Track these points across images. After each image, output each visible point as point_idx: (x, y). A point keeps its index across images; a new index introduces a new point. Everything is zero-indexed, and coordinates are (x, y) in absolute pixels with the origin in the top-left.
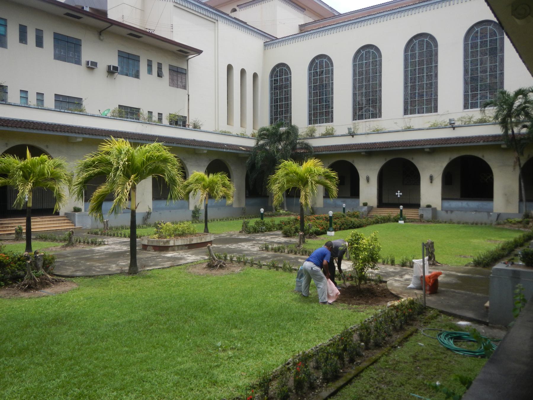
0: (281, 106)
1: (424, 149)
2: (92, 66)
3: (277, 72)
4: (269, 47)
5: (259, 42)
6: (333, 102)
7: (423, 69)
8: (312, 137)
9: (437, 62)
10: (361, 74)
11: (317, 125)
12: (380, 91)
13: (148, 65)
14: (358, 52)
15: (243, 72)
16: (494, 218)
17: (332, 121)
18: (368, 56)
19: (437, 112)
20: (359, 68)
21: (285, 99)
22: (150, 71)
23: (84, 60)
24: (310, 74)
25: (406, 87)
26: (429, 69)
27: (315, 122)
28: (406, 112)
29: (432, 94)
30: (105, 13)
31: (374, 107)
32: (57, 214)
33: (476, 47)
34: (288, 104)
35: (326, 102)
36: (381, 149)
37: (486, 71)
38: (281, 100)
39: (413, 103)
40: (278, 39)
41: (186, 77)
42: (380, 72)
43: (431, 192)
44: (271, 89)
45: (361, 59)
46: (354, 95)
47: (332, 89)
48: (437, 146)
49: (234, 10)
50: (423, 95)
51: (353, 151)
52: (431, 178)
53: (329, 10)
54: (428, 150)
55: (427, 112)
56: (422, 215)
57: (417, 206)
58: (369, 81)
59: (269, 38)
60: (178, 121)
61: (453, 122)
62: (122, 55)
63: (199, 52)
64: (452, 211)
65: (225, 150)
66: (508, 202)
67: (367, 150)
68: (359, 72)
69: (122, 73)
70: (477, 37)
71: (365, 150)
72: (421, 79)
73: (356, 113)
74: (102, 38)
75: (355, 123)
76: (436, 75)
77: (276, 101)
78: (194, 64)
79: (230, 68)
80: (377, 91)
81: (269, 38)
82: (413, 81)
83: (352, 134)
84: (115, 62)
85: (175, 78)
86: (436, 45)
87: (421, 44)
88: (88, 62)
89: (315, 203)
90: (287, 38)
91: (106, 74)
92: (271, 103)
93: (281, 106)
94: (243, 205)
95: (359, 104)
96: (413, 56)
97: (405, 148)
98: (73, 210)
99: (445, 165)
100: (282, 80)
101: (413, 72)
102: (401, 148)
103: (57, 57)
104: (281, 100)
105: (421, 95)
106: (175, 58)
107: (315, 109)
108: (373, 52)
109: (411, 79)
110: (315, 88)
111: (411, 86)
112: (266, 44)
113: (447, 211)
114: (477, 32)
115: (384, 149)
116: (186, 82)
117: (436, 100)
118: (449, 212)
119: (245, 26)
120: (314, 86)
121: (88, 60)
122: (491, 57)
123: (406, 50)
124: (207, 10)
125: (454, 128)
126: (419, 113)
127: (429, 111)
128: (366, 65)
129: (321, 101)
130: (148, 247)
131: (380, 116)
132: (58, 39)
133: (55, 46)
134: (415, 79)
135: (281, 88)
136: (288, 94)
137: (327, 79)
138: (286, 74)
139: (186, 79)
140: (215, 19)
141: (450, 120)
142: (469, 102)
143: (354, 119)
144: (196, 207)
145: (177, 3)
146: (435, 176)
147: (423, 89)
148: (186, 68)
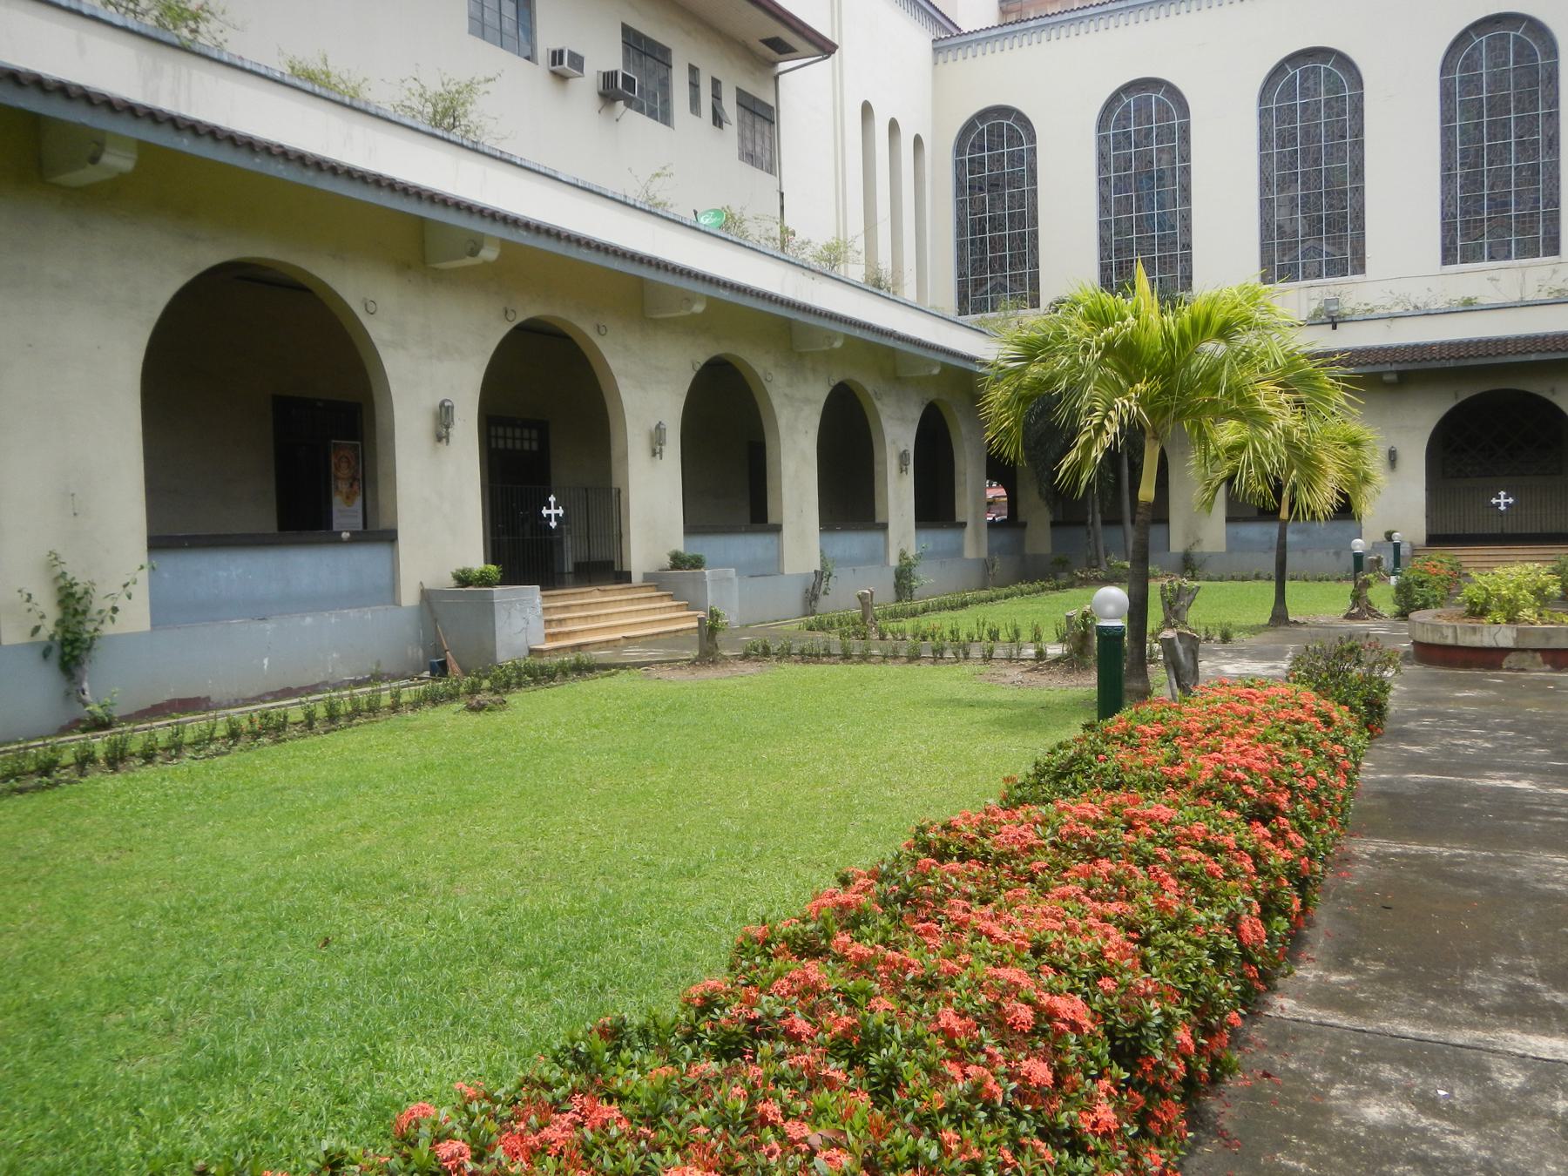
0: (997, 244)
2: (563, 66)
3: (981, 134)
4: (950, 56)
5: (917, 38)
9: (1554, 102)
10: (1286, 138)
12: (1359, 191)
14: (1279, 70)
15: (893, 126)
18: (1310, 83)
20: (1280, 121)
21: (1011, 221)
24: (1102, 140)
25: (1447, 178)
28: (1448, 255)
31: (1338, 243)
32: (624, 577)
34: (1022, 237)
35: (1161, 228)
36: (1462, 363)
38: (997, 223)
42: (1359, 132)
44: (959, 188)
45: (1288, 92)
46: (1265, 205)
47: (1186, 189)
50: (1506, 204)
55: (1519, 256)
58: (1317, 161)
59: (948, 31)
63: (826, 48)
67: (1410, 367)
68: (1279, 132)
71: (1393, 368)
72: (1500, 154)
78: (801, 88)
79: (867, 109)
81: (948, 31)
85: (748, 134)
86: (1551, 49)
87: (1498, 47)
88: (557, 57)
89: (1198, 541)
91: (593, 101)
92: (961, 231)
93: (997, 244)
94: (984, 554)
95: (1282, 234)
96: (1471, 84)
98: (667, 562)
101: (1472, 134)
102: (1533, 357)
104: (997, 223)
108: (1329, 73)
110: (1122, 184)
111: (1466, 177)
112: (940, 44)
115: (1471, 362)
117: (1554, 219)
121: (557, 47)
123: (1446, 68)
126: (1492, 258)
127: (1528, 250)
128: (1304, 110)
130: (1510, 660)
131: (1360, 268)
135: (995, 185)
136: (1022, 206)
137: (1165, 157)
138: (1015, 139)
144: (903, 555)
148: (773, 104)
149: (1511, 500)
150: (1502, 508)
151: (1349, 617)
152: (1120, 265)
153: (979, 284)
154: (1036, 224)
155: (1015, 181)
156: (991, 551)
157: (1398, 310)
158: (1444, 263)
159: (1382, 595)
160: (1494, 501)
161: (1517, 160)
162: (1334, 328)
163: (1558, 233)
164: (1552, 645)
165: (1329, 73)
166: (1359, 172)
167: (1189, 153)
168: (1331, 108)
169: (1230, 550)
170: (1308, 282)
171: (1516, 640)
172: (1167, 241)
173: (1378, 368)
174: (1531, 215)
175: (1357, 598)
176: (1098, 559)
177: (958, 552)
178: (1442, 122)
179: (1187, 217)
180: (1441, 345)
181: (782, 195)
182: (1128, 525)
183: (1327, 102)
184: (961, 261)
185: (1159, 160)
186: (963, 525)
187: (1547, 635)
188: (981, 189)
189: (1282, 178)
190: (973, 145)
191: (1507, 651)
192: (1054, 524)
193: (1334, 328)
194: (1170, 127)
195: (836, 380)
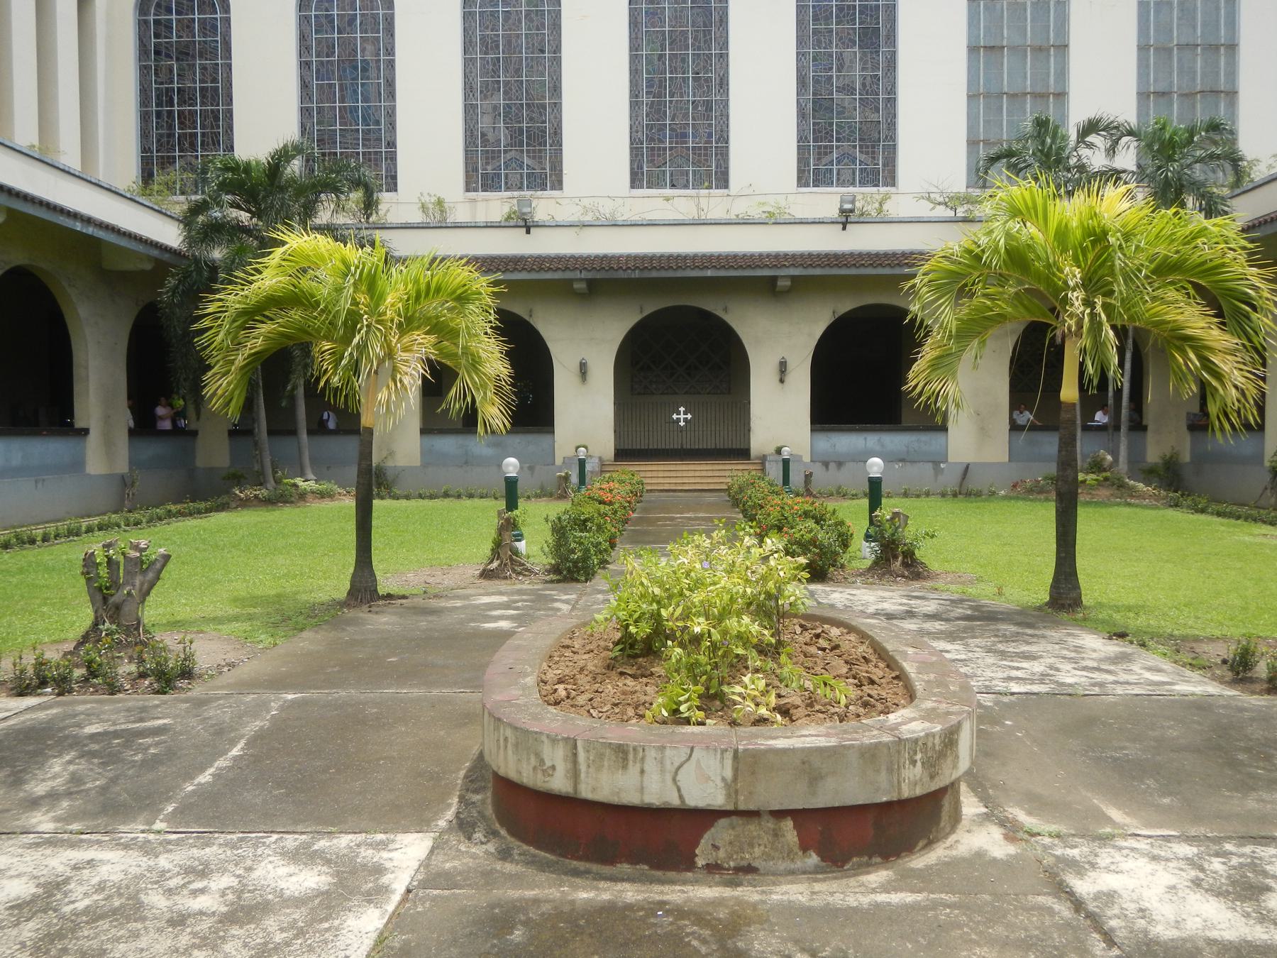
1: (774, 279)
7: (684, 60)
9: (725, 45)
10: (489, 45)
12: (557, 107)
16: (950, 479)
19: (726, 187)
21: (203, 96)
25: (634, 105)
26: (704, 61)
28: (636, 180)
29: (710, 135)
31: (537, 156)
33: (828, 19)
36: (646, 275)
37: (848, 89)
38: (186, 96)
39: (656, 154)
42: (557, 49)
43: (779, 410)
46: (469, 110)
47: (391, 84)
48: (818, 272)
50: (685, 135)
51: (549, 276)
52: (783, 367)
54: (788, 283)
56: (811, 474)
57: (743, 453)
58: (518, 72)
64: (840, 464)
66: (983, 431)
68: (483, 38)
72: (679, 87)
75: (474, 200)
76: (724, 83)
77: (165, 97)
80: (544, 106)
82: (655, 89)
94: (122, 467)
95: (485, 142)
97: (722, 273)
99: (819, 330)
102: (709, 273)
109: (650, 83)
113: (826, 465)
115: (654, 274)
117: (724, 154)
118: (832, 466)
122: (864, 54)
126: (673, 186)
127: (702, 181)
128: (506, 19)
131: (558, 184)
134: (662, 83)
135: (184, 53)
136: (215, 80)
137: (369, 47)
142: (813, 171)
146: (791, 366)
147: (686, 116)
149: (689, 416)
150: (682, 424)
151: (486, 574)
155: (208, 51)
156: (131, 463)
157: (588, 218)
158: (632, 187)
159: (534, 546)
160: (675, 416)
161: (694, 96)
162: (528, 232)
163: (727, 168)
164: (825, 797)
166: (556, 89)
167: (393, 48)
168: (531, 21)
169: (425, 465)
170: (509, 194)
171: (731, 788)
172: (372, 136)
173: (568, 275)
174: (706, 148)
175: (498, 546)
176: (261, 473)
177: (77, 465)
178: (631, 50)
179: (391, 114)
180: (629, 257)
182: (304, 436)
183: (528, 13)
184: (144, 134)
185: (363, 50)
186: (85, 432)
187: (810, 765)
188: (169, 56)
189: (485, 85)
190: (158, 5)
191: (705, 817)
192: (132, 433)
193: (528, 232)
194: (375, 17)
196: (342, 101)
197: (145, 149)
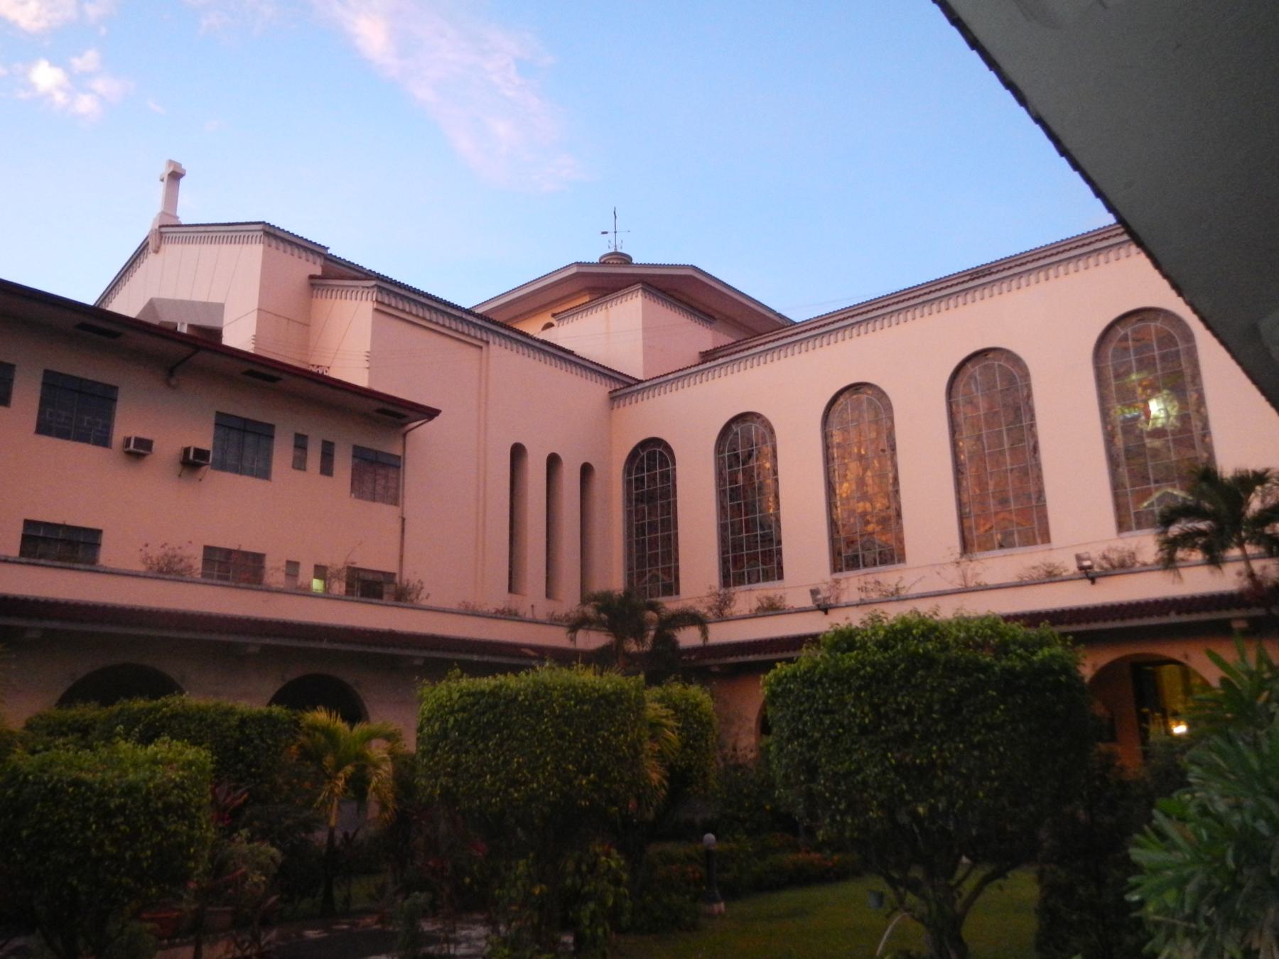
0: (653, 543)
2: (139, 450)
3: (642, 460)
5: (599, 390)
6: (779, 527)
8: (722, 617)
11: (743, 588)
13: (296, 446)
17: (781, 577)
22: (299, 464)
23: (118, 435)
27: (739, 581)
29: (1029, 497)
30: (216, 333)
35: (762, 527)
38: (653, 527)
40: (640, 382)
41: (398, 475)
49: (549, 326)
53: (777, 319)
60: (368, 586)
61: (1087, 563)
62: (224, 423)
63: (430, 413)
65: (475, 658)
69: (222, 466)
70: (1126, 349)
73: (840, 554)
74: (173, 382)
79: (518, 452)
81: (623, 382)
83: (825, 609)
84: (206, 443)
86: (1026, 375)
90: (662, 380)
91: (179, 467)
100: (655, 479)
103: (43, 428)
104: (653, 527)
105: (1002, 498)
106: (371, 428)
107: (737, 546)
114: (1125, 338)
116: (397, 489)
119: (572, 358)
120: (732, 490)
121: (128, 435)
124: (461, 318)
125: (1093, 580)
127: (1029, 541)
129: (750, 525)
132: (54, 385)
133: (43, 403)
135: (651, 497)
136: (669, 513)
139: (398, 479)
140: (482, 340)
141: (1079, 558)
143: (836, 568)
145: (382, 303)
148: (398, 452)
152: (735, 558)
153: (644, 574)
154: (676, 528)
162: (826, 613)
165: (870, 402)
181: (403, 520)
188: (642, 501)
193: (826, 613)
195: (292, 675)
196: (746, 514)
197: (630, 568)
